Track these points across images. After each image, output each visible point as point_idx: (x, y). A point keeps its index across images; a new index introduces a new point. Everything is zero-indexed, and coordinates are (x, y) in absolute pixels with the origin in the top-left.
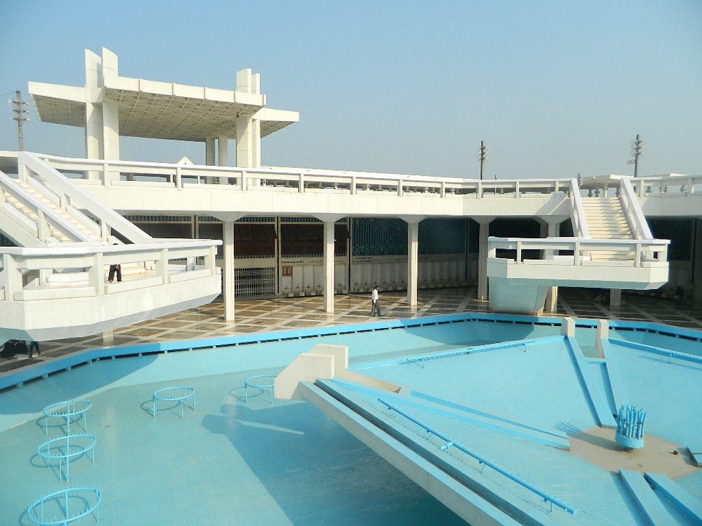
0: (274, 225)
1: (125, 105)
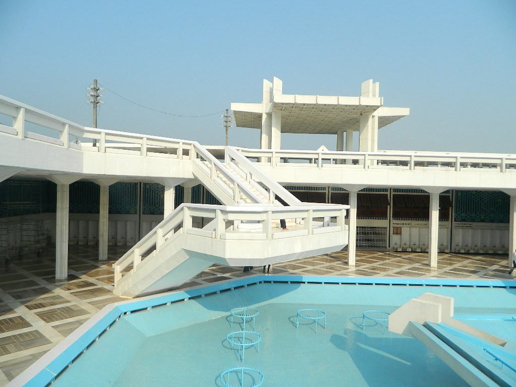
0: (387, 195)
1: (286, 113)
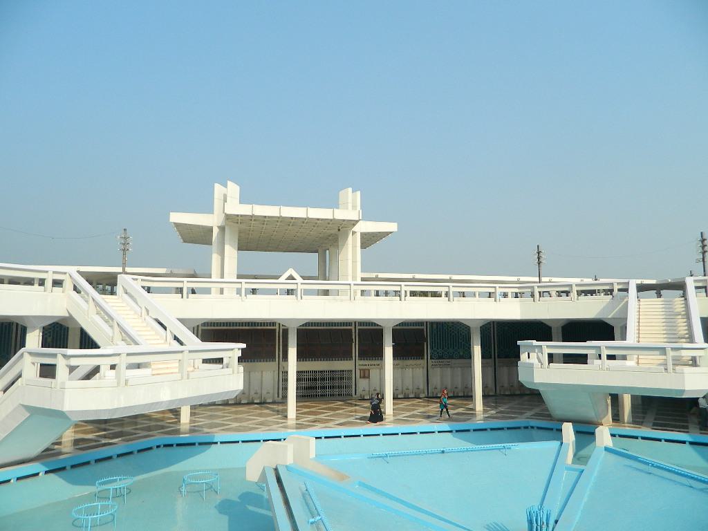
1: (243, 227)
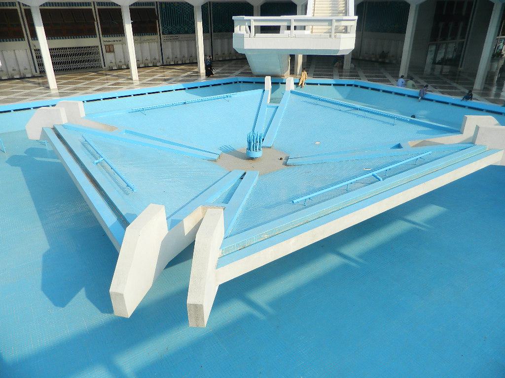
0: (91, 9)
